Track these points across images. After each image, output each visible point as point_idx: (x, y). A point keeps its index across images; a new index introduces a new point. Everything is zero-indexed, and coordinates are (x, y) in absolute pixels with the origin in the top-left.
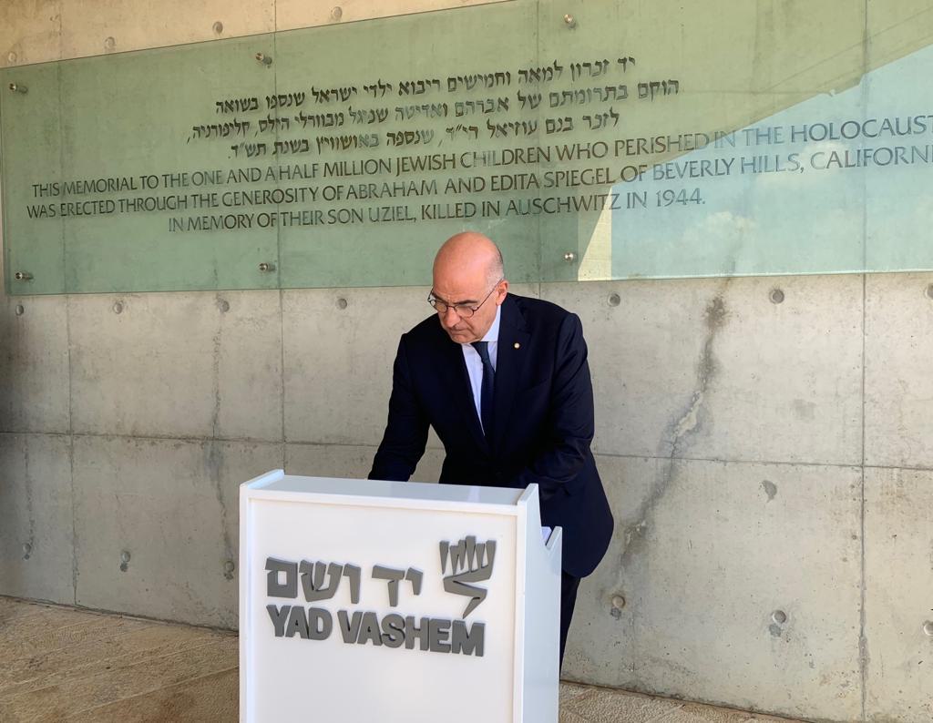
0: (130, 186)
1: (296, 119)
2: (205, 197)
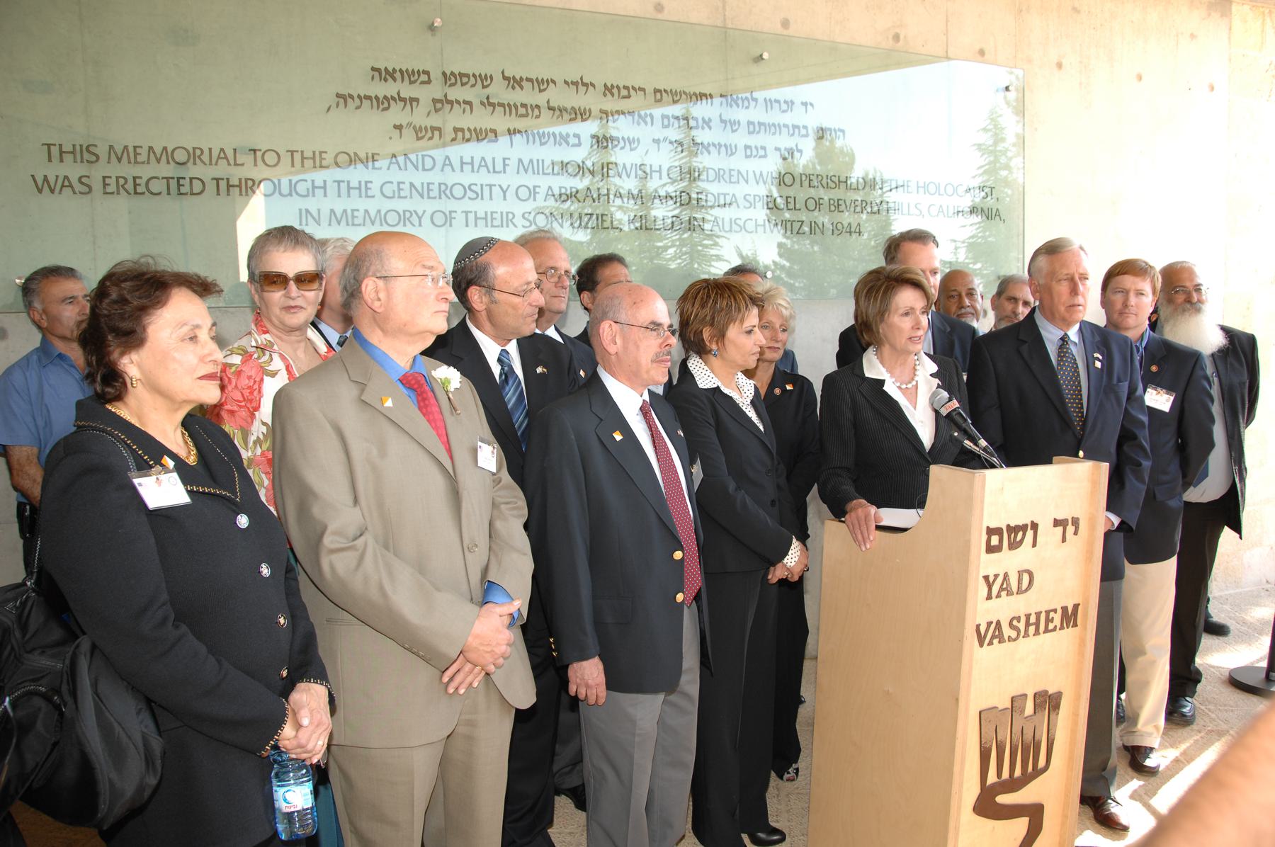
0: (232, 162)
1: (482, 103)
2: (354, 184)
